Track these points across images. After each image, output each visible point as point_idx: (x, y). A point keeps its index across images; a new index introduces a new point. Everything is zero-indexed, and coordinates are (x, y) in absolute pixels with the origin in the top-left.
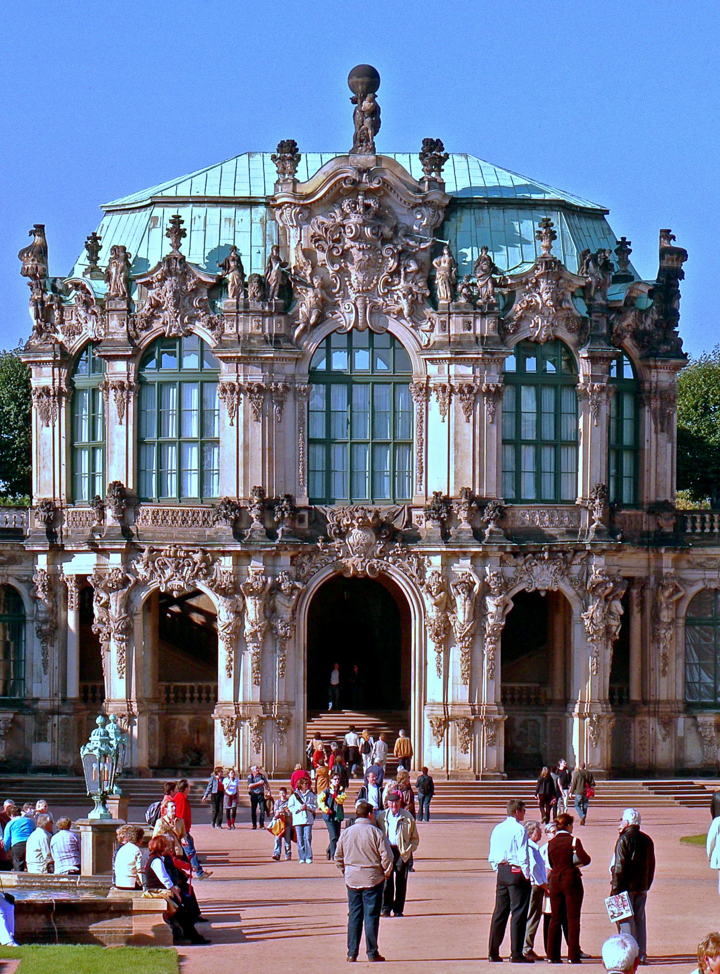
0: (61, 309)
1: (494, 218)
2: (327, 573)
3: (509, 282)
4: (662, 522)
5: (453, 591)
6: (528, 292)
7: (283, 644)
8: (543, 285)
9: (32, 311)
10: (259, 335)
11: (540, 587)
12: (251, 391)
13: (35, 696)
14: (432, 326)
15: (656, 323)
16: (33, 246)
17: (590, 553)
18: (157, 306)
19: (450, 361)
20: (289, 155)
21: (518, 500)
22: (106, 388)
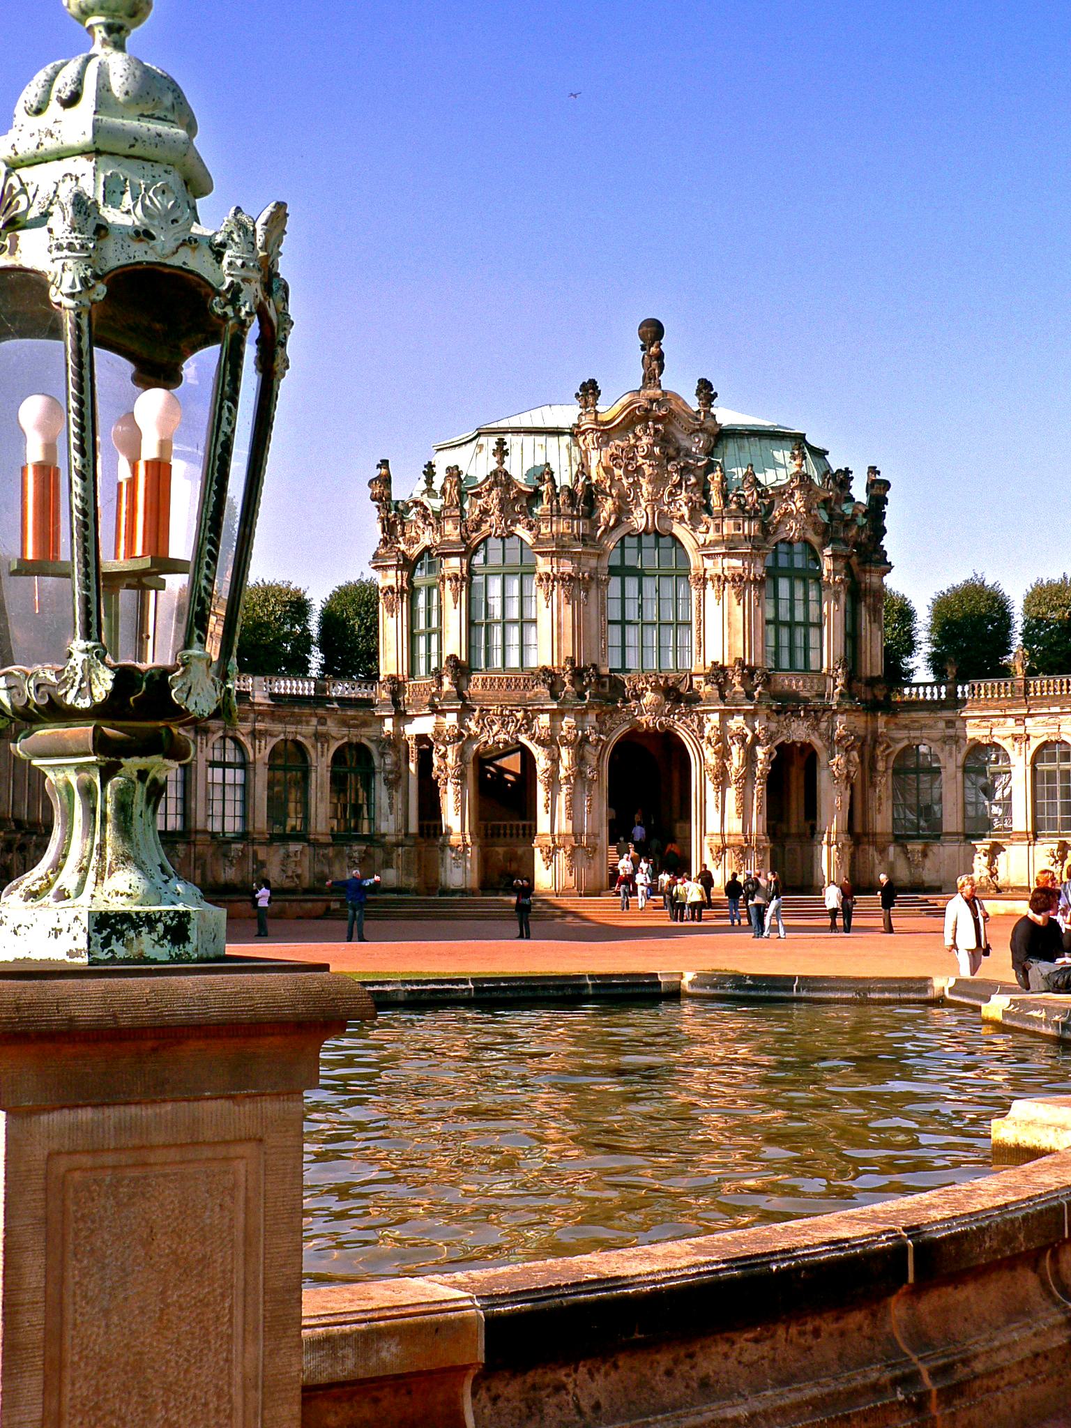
0: (403, 524)
1: (753, 446)
2: (625, 728)
3: (770, 492)
4: (877, 692)
5: (730, 742)
6: (786, 500)
7: (590, 786)
8: (797, 494)
9: (379, 527)
10: (570, 534)
11: (797, 739)
12: (563, 579)
13: (382, 831)
14: (708, 528)
15: (869, 538)
16: (380, 476)
17: (835, 712)
18: (485, 512)
19: (724, 555)
20: (591, 391)
21: (777, 668)
22: (443, 579)
